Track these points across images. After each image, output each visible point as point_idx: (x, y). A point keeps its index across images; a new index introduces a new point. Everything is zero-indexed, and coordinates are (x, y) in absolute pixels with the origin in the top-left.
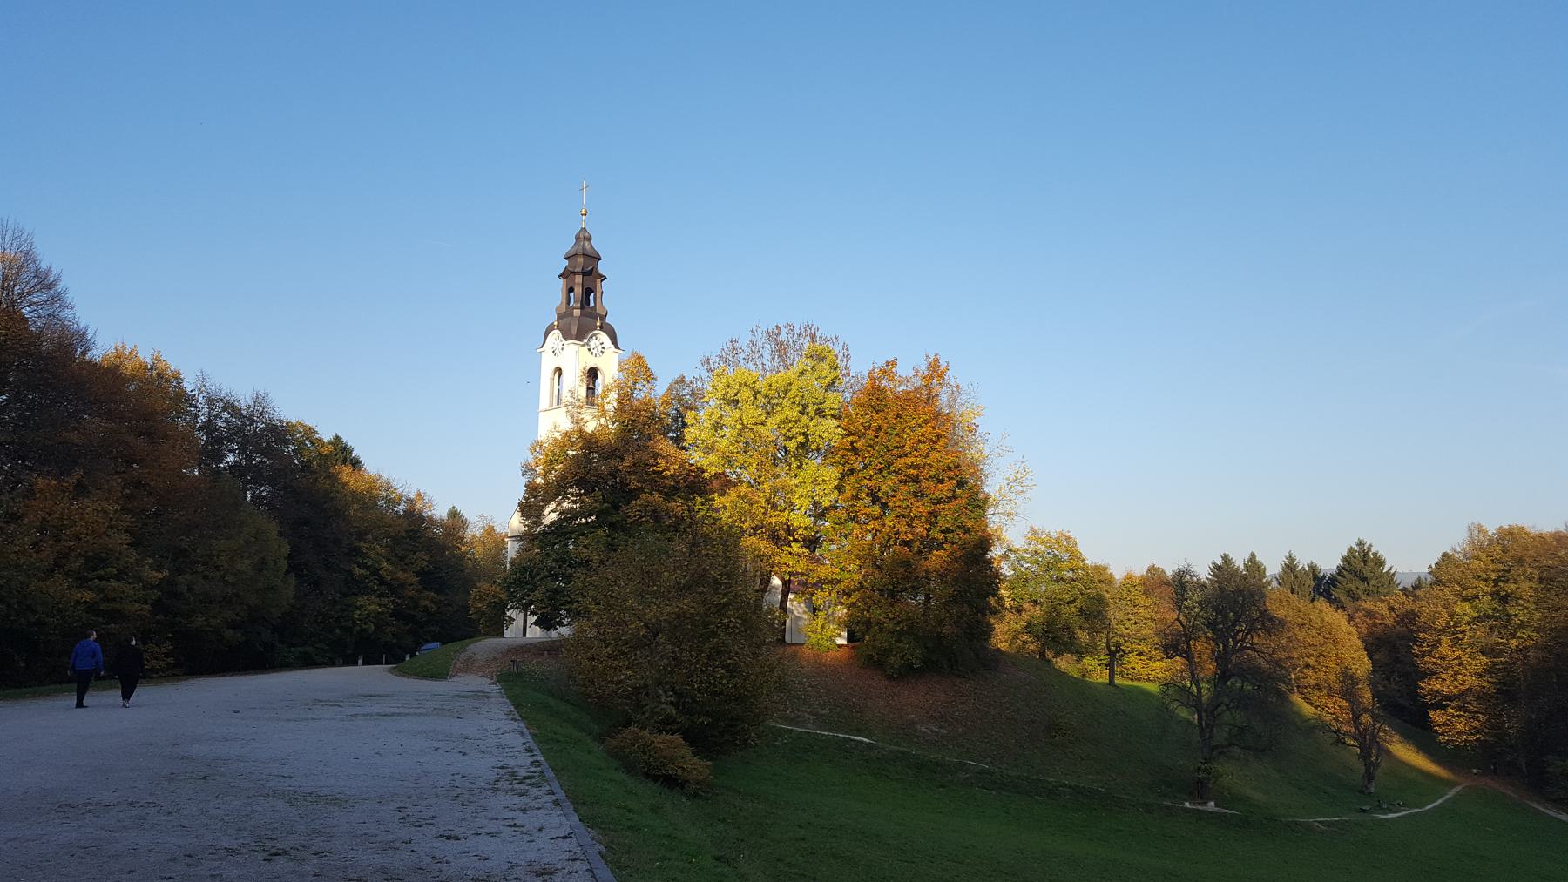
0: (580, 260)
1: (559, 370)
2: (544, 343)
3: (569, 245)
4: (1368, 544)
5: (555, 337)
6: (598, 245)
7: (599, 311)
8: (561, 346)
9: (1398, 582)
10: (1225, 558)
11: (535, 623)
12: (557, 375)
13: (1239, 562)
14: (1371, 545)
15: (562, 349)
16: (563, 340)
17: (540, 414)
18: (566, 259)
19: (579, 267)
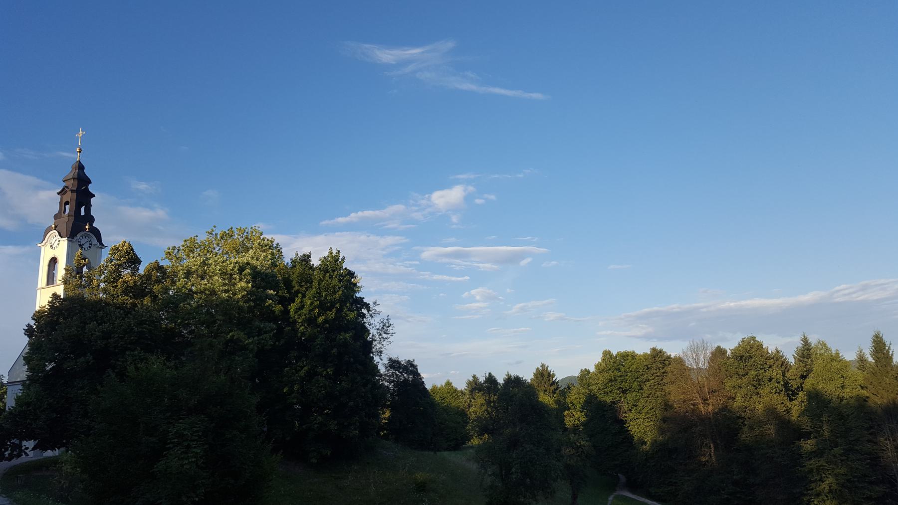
1: (54, 261)
3: (68, 171)
4: (546, 366)
8: (57, 242)
9: (559, 386)
10: (474, 377)
11: (33, 449)
14: (548, 366)
15: (58, 244)
17: (39, 291)
18: (64, 181)
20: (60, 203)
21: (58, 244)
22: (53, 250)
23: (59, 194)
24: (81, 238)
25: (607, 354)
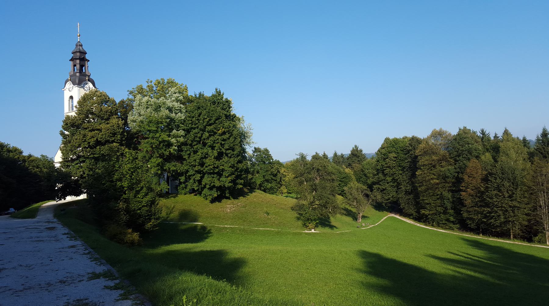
0: (78, 54)
1: (71, 97)
2: (65, 86)
3: (73, 48)
5: (69, 85)
6: (85, 48)
7: (86, 74)
8: (72, 88)
9: (366, 157)
12: (71, 99)
13: (321, 154)
15: (73, 89)
16: (73, 85)
18: (72, 53)
19: (78, 57)
20: (72, 67)
21: (73, 89)
22: (70, 92)
23: (70, 60)
24: (84, 85)
25: (387, 140)
